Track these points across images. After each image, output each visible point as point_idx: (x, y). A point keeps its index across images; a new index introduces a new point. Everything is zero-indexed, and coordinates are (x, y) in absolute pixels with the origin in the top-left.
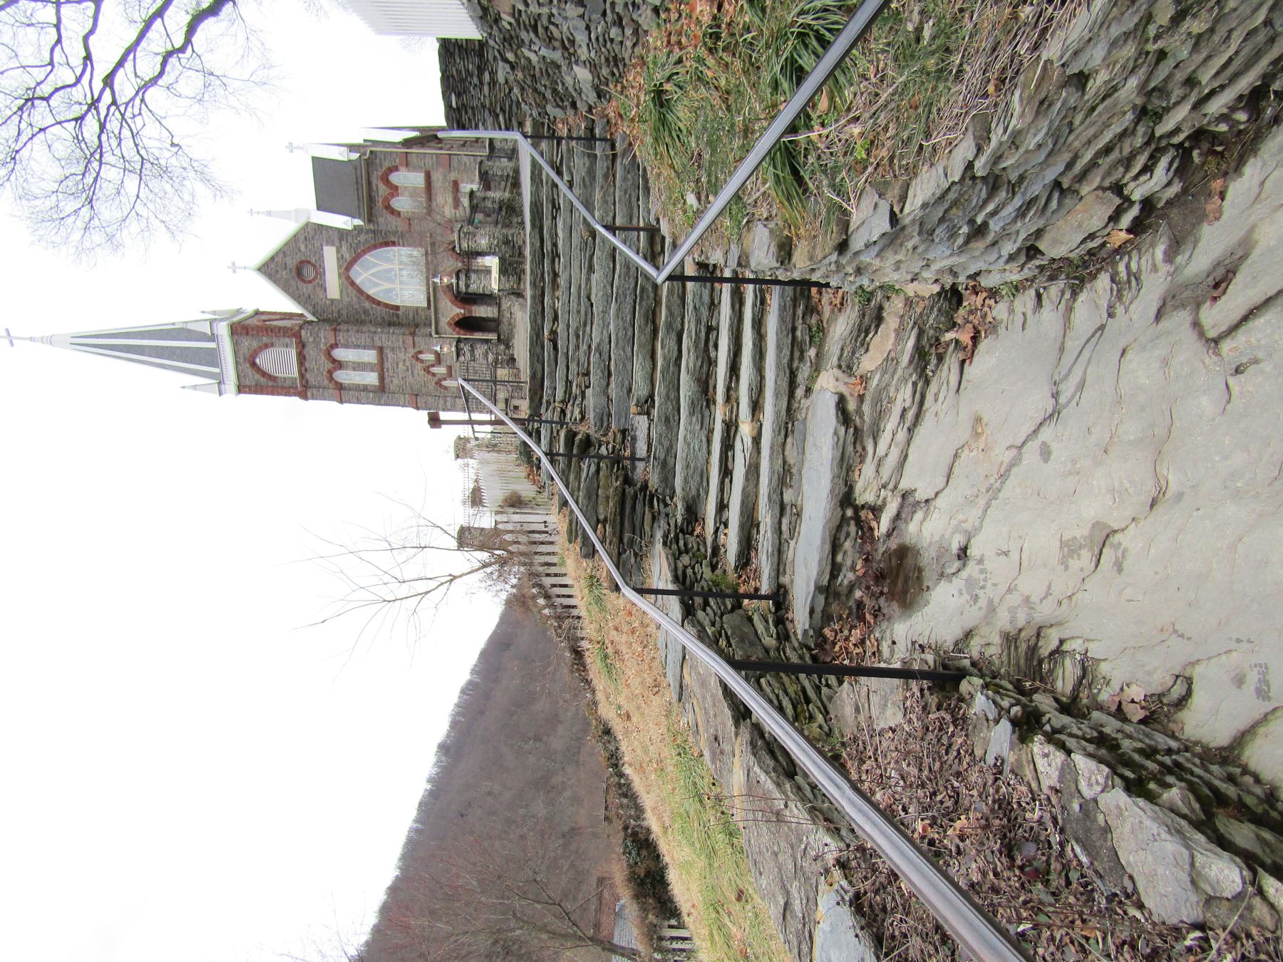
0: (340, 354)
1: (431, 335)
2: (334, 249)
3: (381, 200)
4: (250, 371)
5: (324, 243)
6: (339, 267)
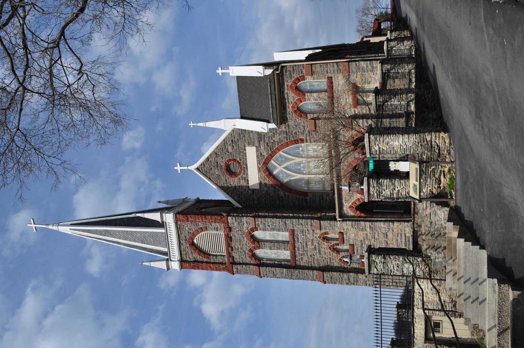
0: (258, 234)
2: (254, 149)
3: (291, 106)
4: (189, 250)
5: (246, 145)
6: (259, 162)
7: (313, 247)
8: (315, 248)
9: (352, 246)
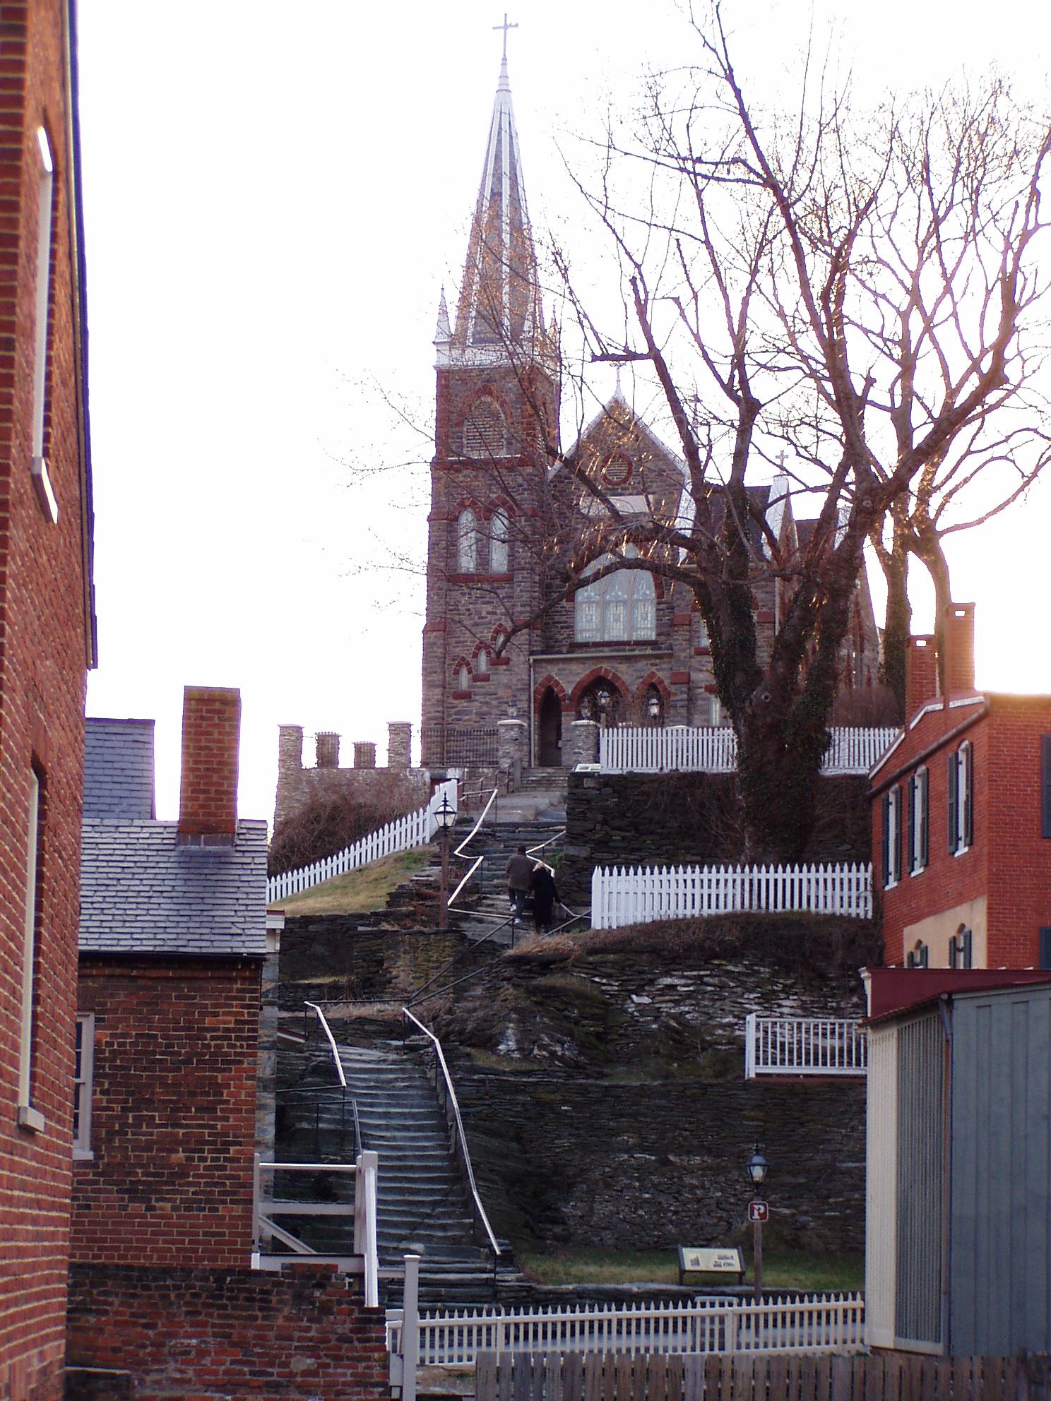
1: (532, 653)
7: (484, 614)
8: (483, 618)
9: (486, 678)
